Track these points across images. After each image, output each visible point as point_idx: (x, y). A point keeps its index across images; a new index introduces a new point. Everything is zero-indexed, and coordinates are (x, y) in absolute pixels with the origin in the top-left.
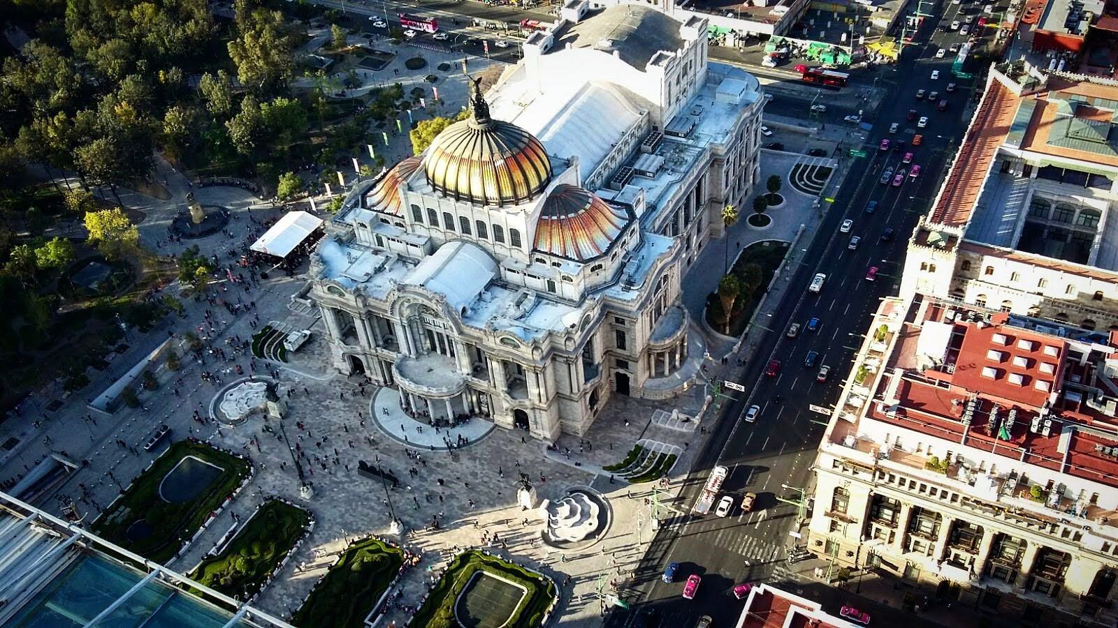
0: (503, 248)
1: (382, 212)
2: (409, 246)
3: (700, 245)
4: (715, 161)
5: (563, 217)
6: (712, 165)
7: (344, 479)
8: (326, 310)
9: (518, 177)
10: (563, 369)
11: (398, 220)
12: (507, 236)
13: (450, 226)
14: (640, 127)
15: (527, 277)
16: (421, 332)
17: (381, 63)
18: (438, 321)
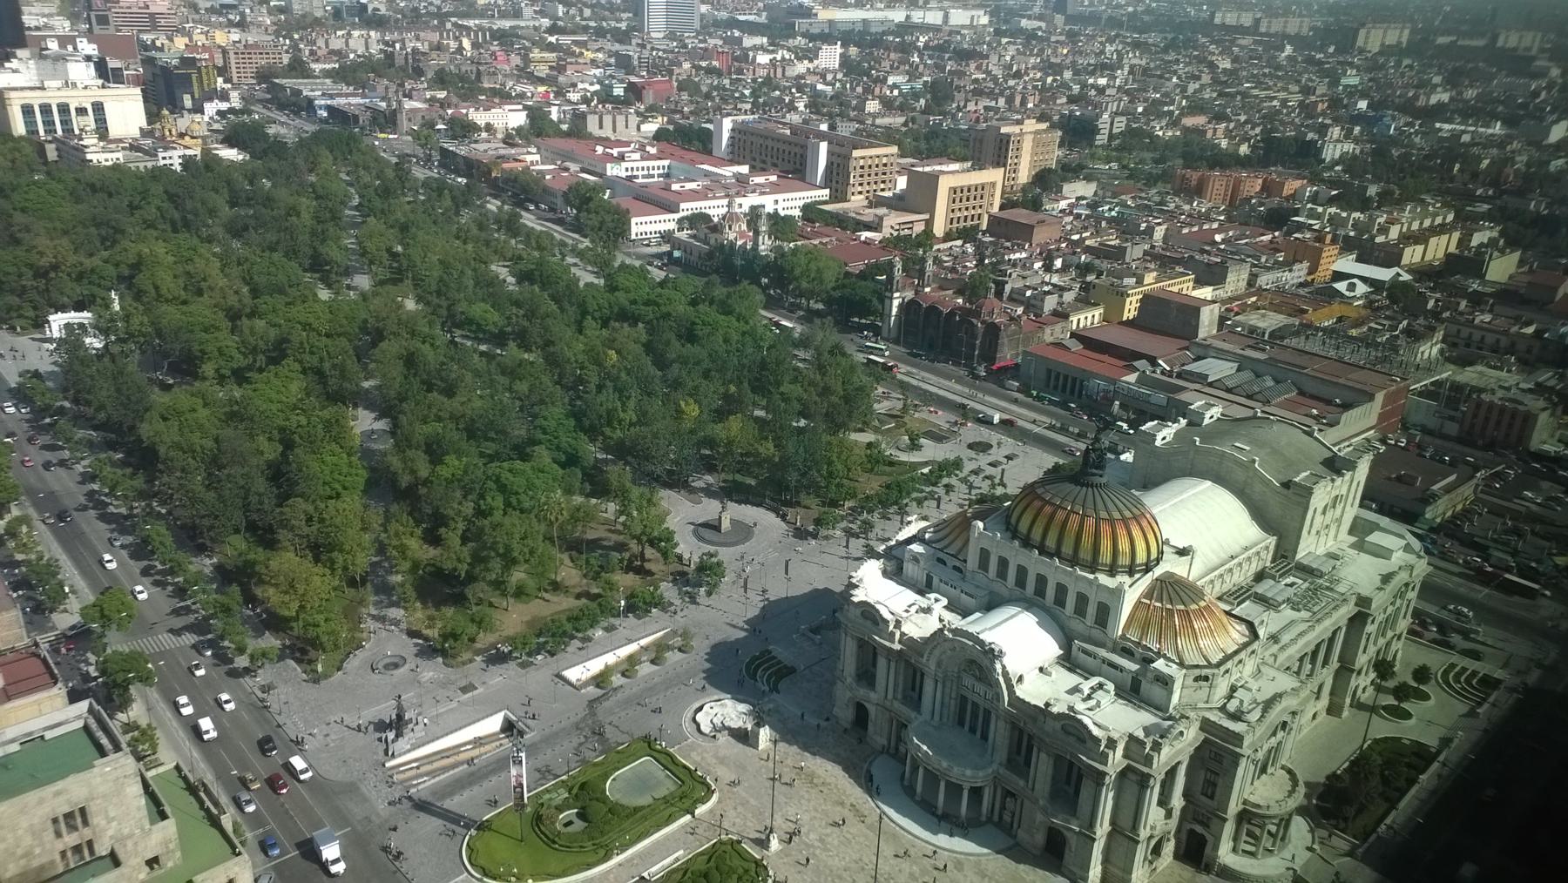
0: (1081, 625)
1: (941, 550)
2: (963, 595)
3: (1314, 717)
4: (1358, 620)
5: (1169, 606)
6: (1351, 620)
7: (817, 844)
8: (849, 639)
9: (1124, 545)
10: (1131, 789)
11: (958, 564)
12: (1091, 610)
13: (1021, 582)
14: (1267, 548)
15: (1105, 666)
16: (953, 696)
17: (946, 438)
18: (980, 688)
